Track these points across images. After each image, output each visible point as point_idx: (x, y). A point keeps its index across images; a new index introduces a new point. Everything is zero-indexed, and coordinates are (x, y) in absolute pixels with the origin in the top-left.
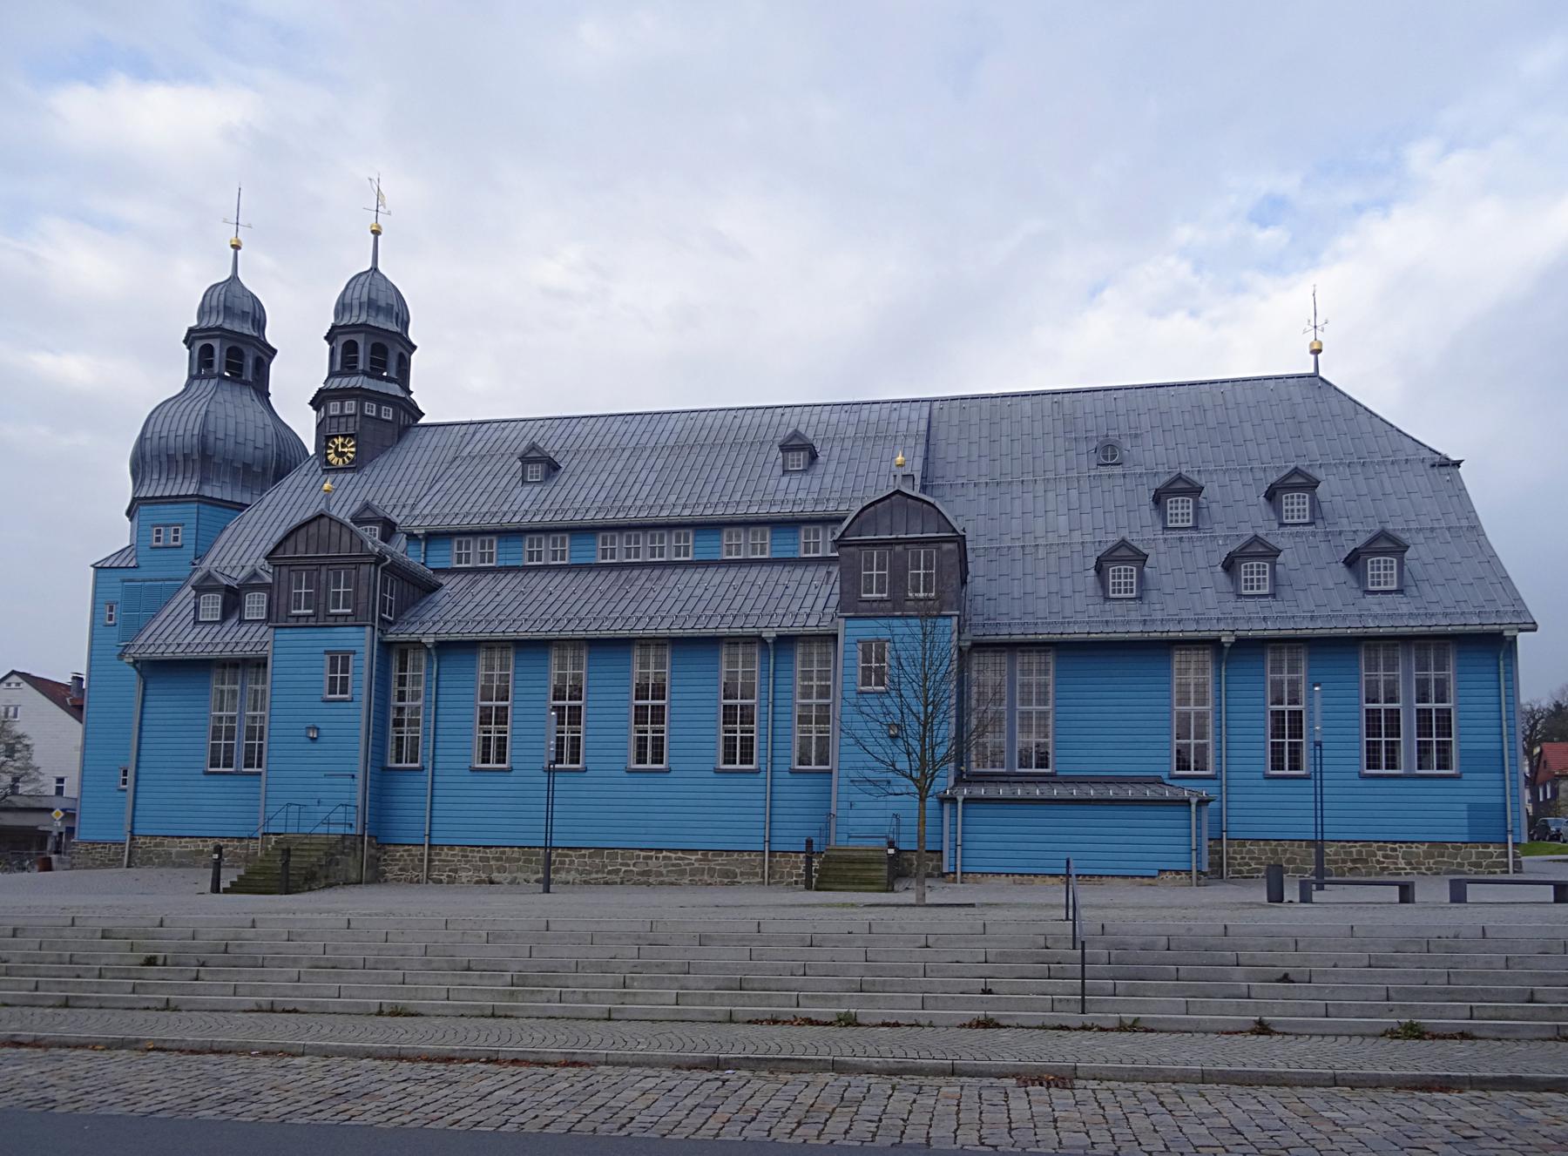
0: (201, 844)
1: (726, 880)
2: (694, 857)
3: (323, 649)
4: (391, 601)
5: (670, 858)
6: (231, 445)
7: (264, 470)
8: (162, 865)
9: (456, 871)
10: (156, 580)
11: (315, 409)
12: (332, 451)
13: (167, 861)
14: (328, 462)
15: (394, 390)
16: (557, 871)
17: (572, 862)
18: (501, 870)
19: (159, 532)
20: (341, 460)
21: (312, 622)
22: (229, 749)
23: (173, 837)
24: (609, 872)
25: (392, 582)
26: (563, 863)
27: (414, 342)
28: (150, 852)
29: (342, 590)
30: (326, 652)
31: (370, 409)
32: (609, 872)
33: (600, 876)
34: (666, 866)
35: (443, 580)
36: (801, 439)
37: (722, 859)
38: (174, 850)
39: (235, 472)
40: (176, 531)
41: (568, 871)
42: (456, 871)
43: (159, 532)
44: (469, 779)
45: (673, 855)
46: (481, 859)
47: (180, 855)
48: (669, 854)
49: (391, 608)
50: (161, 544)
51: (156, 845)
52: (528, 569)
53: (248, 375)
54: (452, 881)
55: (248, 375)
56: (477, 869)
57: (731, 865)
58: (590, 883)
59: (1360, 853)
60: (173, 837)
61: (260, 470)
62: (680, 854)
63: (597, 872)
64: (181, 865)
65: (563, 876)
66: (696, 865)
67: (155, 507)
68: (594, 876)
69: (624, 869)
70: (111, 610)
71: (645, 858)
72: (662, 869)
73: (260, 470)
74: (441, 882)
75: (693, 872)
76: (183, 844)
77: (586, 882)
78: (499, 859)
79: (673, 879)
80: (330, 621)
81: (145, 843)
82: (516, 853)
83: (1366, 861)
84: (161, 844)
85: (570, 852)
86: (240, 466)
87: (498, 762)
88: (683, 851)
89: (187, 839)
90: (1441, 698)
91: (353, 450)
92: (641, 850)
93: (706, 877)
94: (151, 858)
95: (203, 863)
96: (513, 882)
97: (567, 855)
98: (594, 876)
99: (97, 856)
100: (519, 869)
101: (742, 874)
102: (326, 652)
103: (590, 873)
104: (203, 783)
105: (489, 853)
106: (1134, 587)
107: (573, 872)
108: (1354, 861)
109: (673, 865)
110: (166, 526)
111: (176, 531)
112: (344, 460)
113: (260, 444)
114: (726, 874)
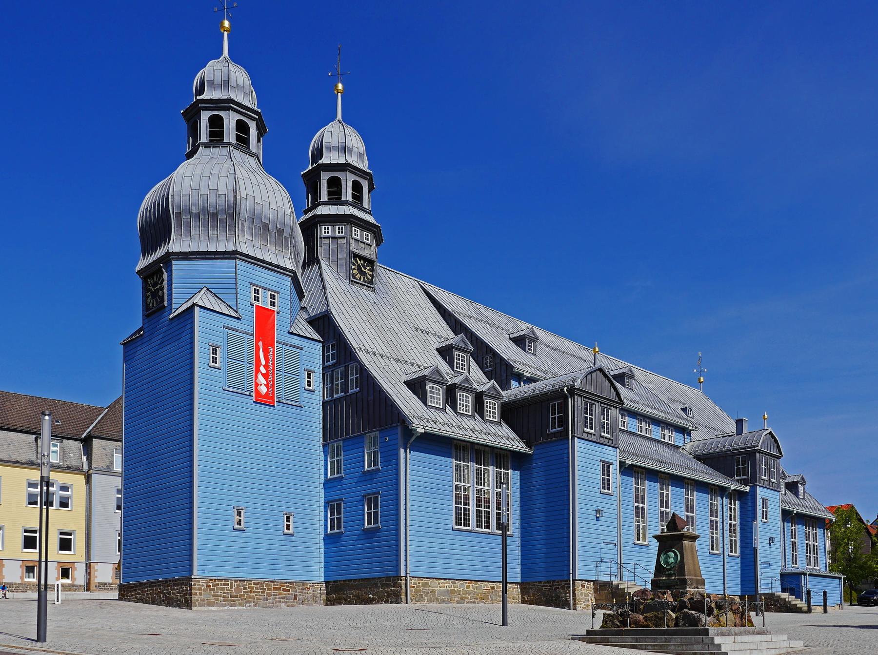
3: (599, 459)
12: (356, 268)
23: (434, 578)
29: (557, 415)
30: (601, 461)
44: (633, 549)
47: (441, 594)
60: (434, 578)
67: (251, 266)
76: (441, 585)
81: (415, 583)
84: (426, 585)
89: (442, 581)
95: (456, 599)
102: (601, 461)
112: (364, 278)
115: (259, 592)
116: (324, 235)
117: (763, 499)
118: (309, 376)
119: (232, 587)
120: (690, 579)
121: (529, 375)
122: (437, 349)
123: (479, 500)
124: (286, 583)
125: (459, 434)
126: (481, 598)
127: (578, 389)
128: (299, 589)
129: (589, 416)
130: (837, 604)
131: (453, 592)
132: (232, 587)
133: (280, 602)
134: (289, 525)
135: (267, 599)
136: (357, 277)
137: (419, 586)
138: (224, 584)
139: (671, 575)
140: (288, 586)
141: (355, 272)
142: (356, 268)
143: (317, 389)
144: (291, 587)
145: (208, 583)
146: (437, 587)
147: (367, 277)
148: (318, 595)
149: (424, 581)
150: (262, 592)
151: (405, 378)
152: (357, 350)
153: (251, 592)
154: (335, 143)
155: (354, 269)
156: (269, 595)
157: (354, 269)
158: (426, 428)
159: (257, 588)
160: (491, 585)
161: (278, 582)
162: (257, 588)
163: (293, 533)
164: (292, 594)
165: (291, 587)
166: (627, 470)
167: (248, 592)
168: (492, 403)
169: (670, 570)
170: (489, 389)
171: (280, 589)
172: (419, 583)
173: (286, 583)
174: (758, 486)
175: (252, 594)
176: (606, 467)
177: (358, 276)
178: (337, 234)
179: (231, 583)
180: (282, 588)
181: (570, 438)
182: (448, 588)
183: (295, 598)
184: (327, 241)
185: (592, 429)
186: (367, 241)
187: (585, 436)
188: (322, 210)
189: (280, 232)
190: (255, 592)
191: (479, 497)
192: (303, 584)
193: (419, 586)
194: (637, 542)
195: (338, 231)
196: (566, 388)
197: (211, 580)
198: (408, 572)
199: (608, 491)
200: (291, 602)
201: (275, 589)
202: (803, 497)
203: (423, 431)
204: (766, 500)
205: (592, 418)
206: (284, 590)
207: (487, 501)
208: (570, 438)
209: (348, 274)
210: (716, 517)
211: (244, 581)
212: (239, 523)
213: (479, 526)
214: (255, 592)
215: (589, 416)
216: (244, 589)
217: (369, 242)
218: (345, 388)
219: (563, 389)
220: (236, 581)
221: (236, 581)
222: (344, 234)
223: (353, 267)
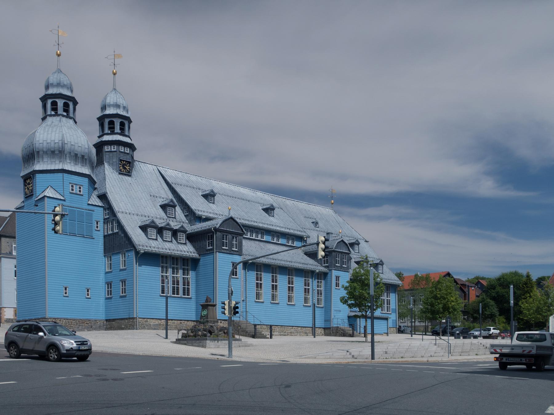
0: (160, 321)
1: (306, 335)
2: (299, 328)
3: (231, 261)
8: (149, 329)
10: (73, 207)
12: (121, 166)
13: (150, 328)
14: (120, 170)
16: (274, 332)
20: (125, 171)
21: (228, 252)
22: (178, 288)
24: (284, 332)
26: (275, 330)
28: (144, 324)
31: (122, 149)
32: (284, 332)
34: (295, 331)
37: (304, 329)
38: (152, 323)
44: (255, 304)
47: (154, 325)
48: (295, 327)
58: (281, 335)
60: (150, 319)
62: (297, 328)
63: (282, 332)
64: (155, 329)
65: (275, 333)
68: (282, 333)
69: (287, 331)
72: (294, 331)
75: (300, 332)
80: (232, 252)
81: (141, 321)
84: (147, 321)
85: (276, 327)
91: (129, 167)
93: (302, 334)
94: (144, 327)
95: (162, 328)
97: (275, 328)
98: (282, 333)
102: (232, 262)
103: (281, 332)
104: (160, 299)
106: (184, 240)
107: (277, 332)
110: (76, 185)
111: (80, 188)
112: (126, 171)
114: (306, 333)
115: (75, 324)
116: (106, 150)
117: (336, 277)
118: (97, 224)
119: (63, 322)
120: (210, 320)
121: (205, 217)
122: (160, 206)
123: (174, 282)
124: (87, 320)
125: (162, 251)
126: (174, 328)
127: (218, 229)
128: (93, 323)
129: (225, 241)
130: (385, 333)
131: (160, 325)
132: (63, 322)
133: (84, 329)
134: (89, 294)
135: (79, 328)
136: (122, 170)
137: (143, 322)
138: (59, 321)
139: (204, 319)
140: (88, 322)
141: (121, 168)
142: (121, 166)
143: (101, 229)
144: (89, 322)
145: (52, 320)
146: (152, 322)
147: (127, 170)
148: (102, 326)
149: (145, 320)
150: (76, 324)
151: (140, 224)
152: (117, 212)
153: (72, 324)
154: (112, 103)
155: (121, 167)
156: (80, 326)
157: (121, 167)
158: (145, 250)
159: (74, 323)
160: (179, 322)
161: (83, 320)
162: (74, 323)
163: (90, 297)
164: (90, 325)
165: (89, 322)
166: (247, 265)
167: (70, 324)
168: (182, 234)
169: (204, 317)
170: (180, 228)
171: (84, 323)
172: (143, 321)
173: (87, 320)
174: (333, 270)
175: (72, 325)
176: (235, 265)
177: (123, 170)
178: (113, 150)
179: (63, 320)
180: (85, 322)
181: (215, 252)
182: (158, 323)
183: (91, 327)
184: (108, 153)
185: (227, 247)
186: (127, 152)
187: (223, 251)
188: (106, 138)
190: (73, 324)
191: (174, 280)
192: (95, 321)
193: (143, 322)
194: (256, 300)
195: (114, 148)
196: (213, 228)
197: (54, 319)
198: (137, 315)
199: (236, 277)
200: (90, 329)
201: (82, 323)
202: (381, 272)
203: (143, 252)
204: (339, 277)
205: (227, 242)
206: (86, 323)
207: (178, 282)
208: (215, 252)
209: (118, 169)
210: (308, 286)
211: (68, 319)
212: (66, 293)
213: (174, 294)
214: (73, 324)
215: (225, 241)
216: (69, 323)
217: (128, 152)
218: (112, 230)
219: (211, 229)
220: (64, 319)
221: (64, 319)
222: (115, 150)
223: (120, 166)
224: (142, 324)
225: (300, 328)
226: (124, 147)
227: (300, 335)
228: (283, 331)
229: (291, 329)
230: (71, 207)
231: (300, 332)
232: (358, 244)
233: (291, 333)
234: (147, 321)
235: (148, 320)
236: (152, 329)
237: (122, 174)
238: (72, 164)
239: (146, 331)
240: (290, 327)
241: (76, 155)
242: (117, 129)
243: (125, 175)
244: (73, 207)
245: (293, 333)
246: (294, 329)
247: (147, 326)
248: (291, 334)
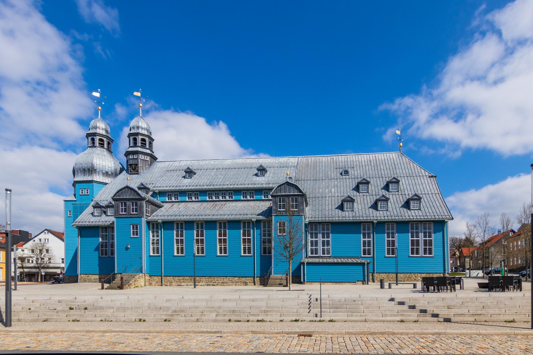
4: (149, 210)
5: (229, 279)
6: (101, 166)
7: (112, 173)
8: (89, 282)
9: (171, 283)
10: (82, 204)
11: (126, 157)
15: (148, 151)
17: (203, 280)
18: (184, 282)
19: (82, 191)
24: (213, 283)
25: (149, 205)
26: (201, 280)
27: (153, 138)
32: (213, 283)
33: (211, 283)
34: (228, 281)
35: (164, 204)
36: (262, 167)
39: (103, 174)
40: (87, 190)
41: (202, 282)
42: (171, 283)
43: (82, 191)
45: (230, 278)
46: (178, 279)
47: (94, 279)
49: (149, 212)
50: (83, 194)
51: (87, 277)
52: (187, 202)
53: (106, 146)
54: (170, 285)
55: (106, 146)
56: (177, 282)
57: (246, 280)
59: (409, 276)
61: (110, 173)
63: (210, 283)
66: (237, 280)
69: (217, 281)
70: (70, 212)
71: (223, 279)
73: (110, 173)
74: (167, 285)
77: (208, 285)
78: (183, 279)
79: (231, 284)
82: (188, 278)
83: (410, 278)
84: (89, 276)
86: (105, 172)
87: (182, 254)
88: (233, 277)
90: (430, 237)
92: (222, 277)
94: (86, 280)
96: (187, 285)
97: (202, 278)
99: (71, 280)
100: (189, 282)
101: (249, 283)
105: (180, 278)
108: (407, 278)
109: (231, 280)
111: (87, 190)
113: (110, 166)
189: (89, 169)
224: (84, 279)
225: (236, 278)
226: (133, 155)
227: (236, 285)
228: (212, 281)
229: (223, 279)
230: (81, 204)
231: (236, 282)
232: (397, 182)
233: (223, 283)
234: (89, 276)
235: (90, 276)
236: (92, 282)
237: (132, 174)
238: (82, 176)
239: (87, 283)
240: (222, 278)
241: (84, 170)
242: (139, 144)
243: (134, 174)
244: (82, 204)
245: (227, 283)
246: (228, 279)
247: (88, 280)
248: (223, 284)
